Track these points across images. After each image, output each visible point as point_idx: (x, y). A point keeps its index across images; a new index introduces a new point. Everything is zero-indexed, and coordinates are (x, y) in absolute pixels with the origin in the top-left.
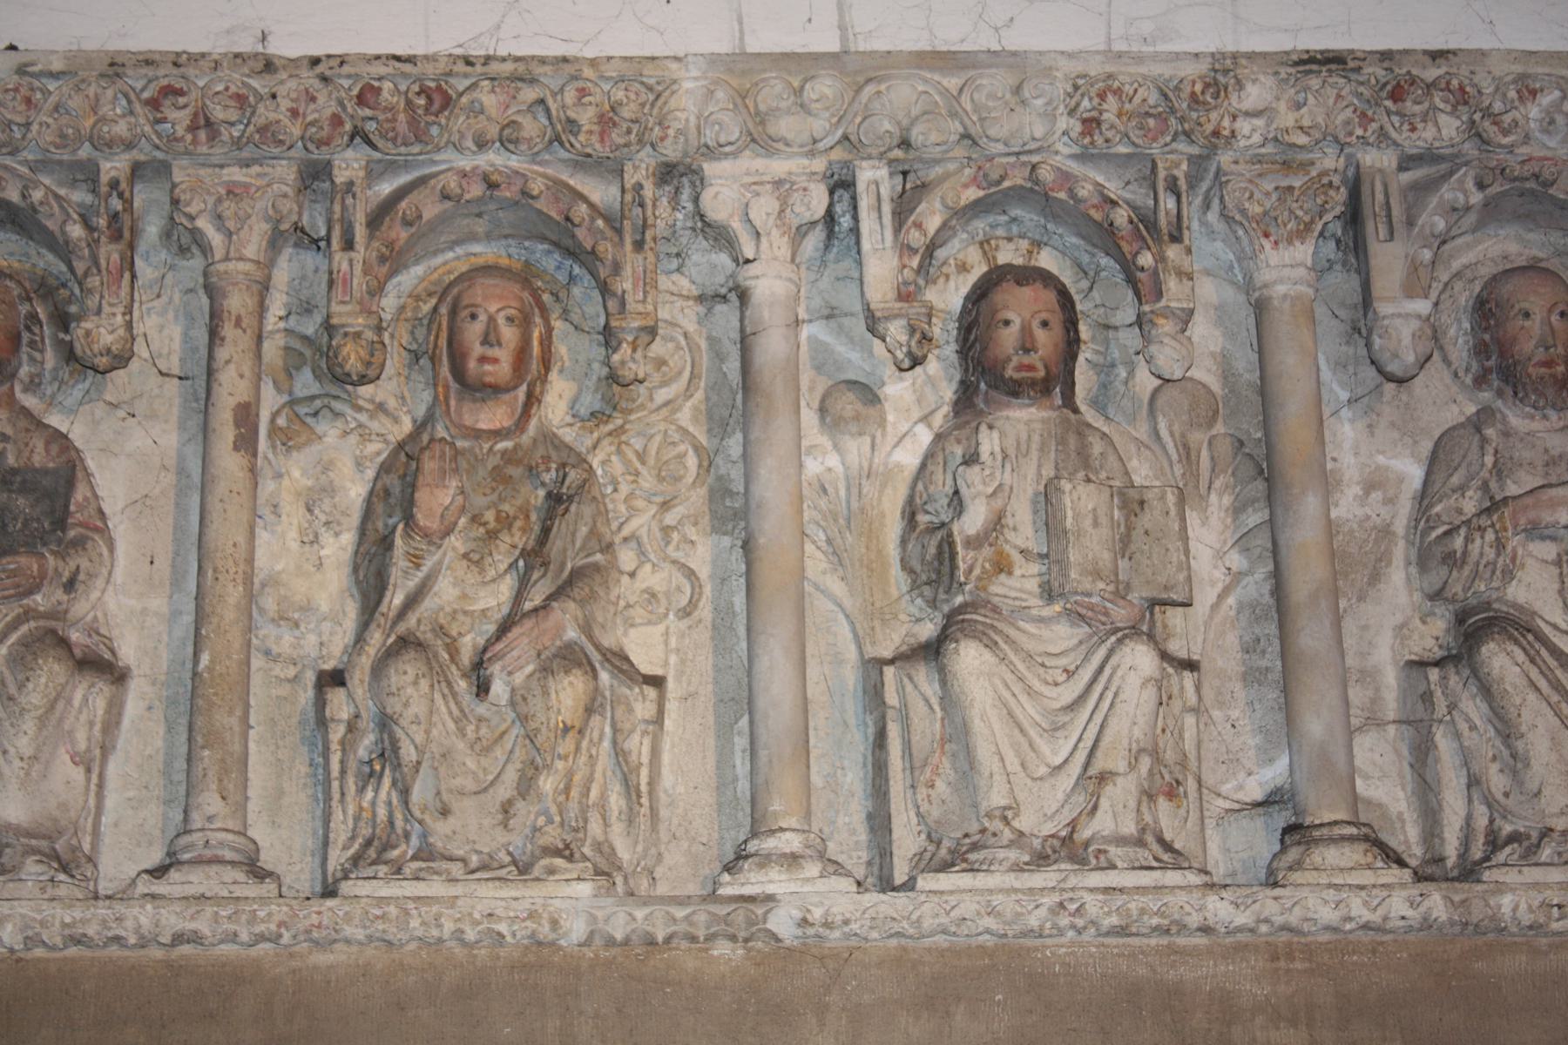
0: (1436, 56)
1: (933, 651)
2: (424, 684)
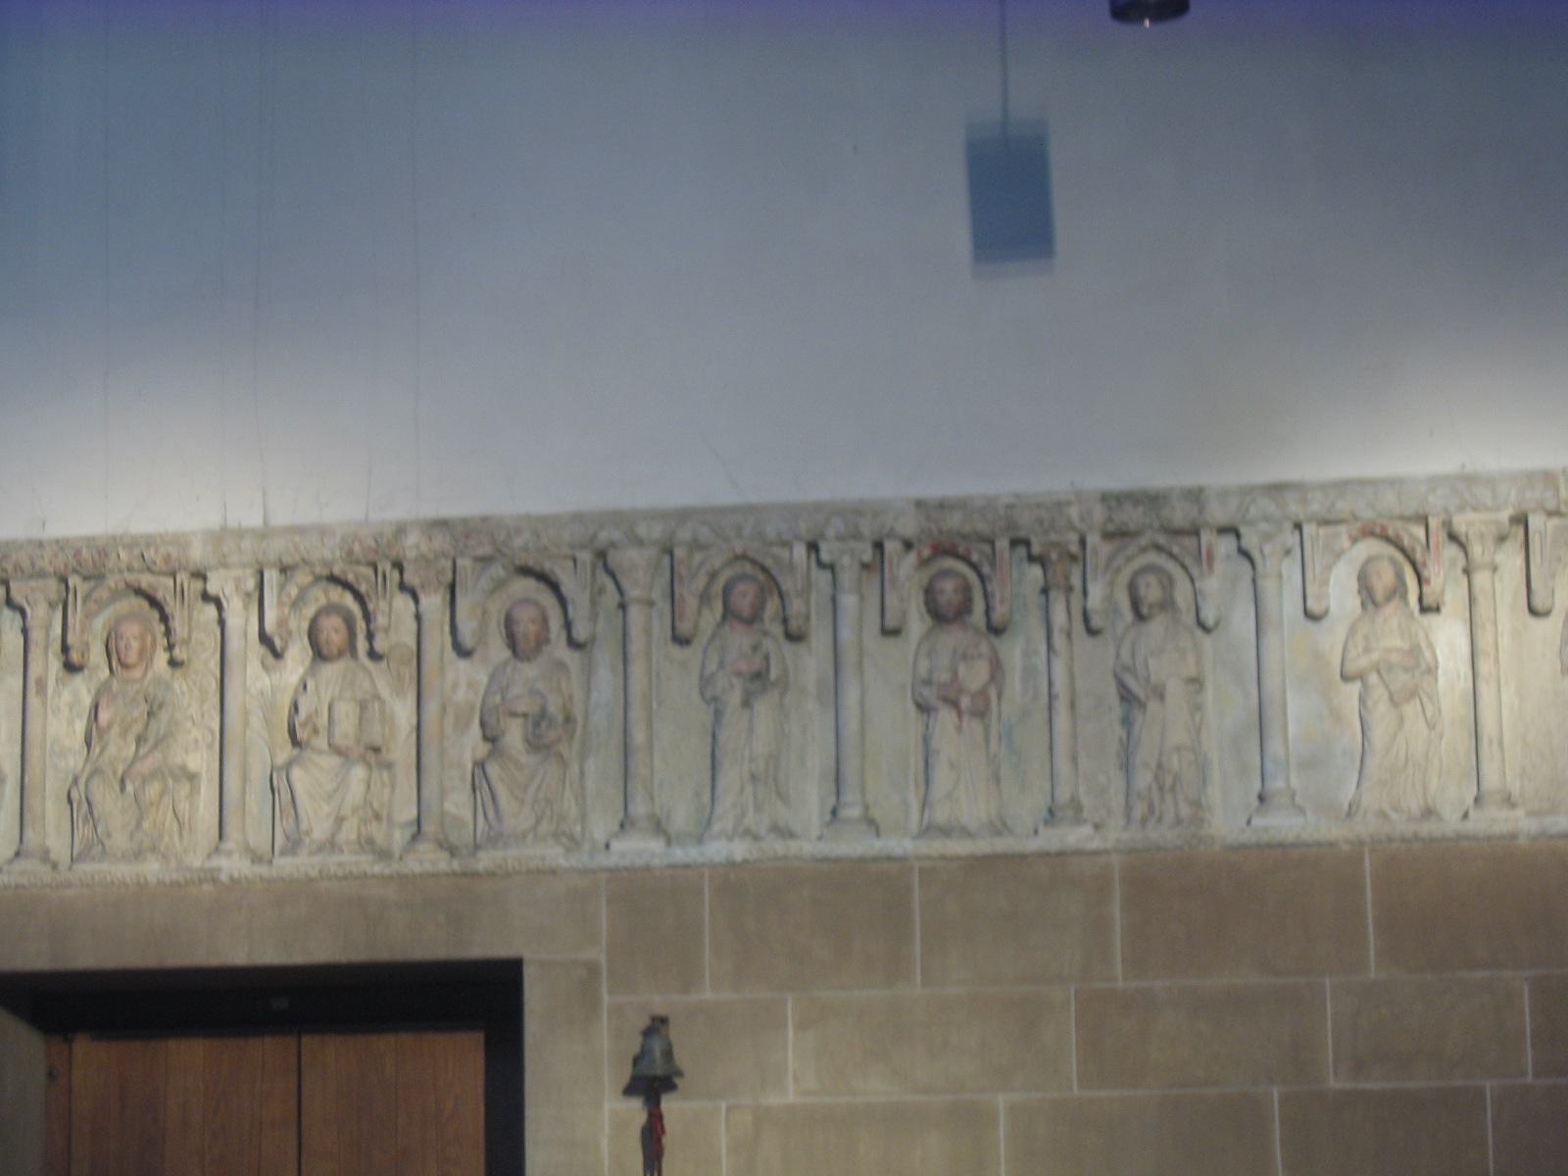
1: (288, 766)
2: (101, 788)
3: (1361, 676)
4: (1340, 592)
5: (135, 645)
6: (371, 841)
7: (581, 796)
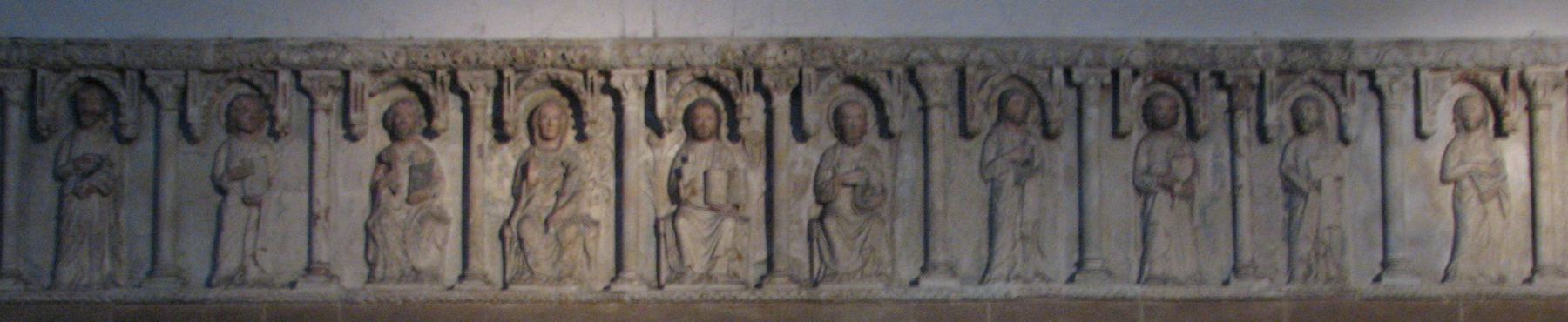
0: (826, 39)
3: (1456, 182)
4: (1441, 122)
5: (555, 122)
6: (735, 275)
7: (892, 246)
